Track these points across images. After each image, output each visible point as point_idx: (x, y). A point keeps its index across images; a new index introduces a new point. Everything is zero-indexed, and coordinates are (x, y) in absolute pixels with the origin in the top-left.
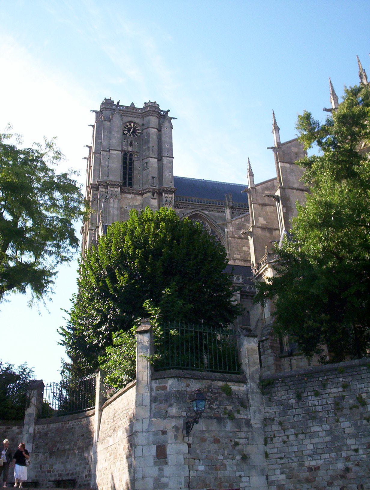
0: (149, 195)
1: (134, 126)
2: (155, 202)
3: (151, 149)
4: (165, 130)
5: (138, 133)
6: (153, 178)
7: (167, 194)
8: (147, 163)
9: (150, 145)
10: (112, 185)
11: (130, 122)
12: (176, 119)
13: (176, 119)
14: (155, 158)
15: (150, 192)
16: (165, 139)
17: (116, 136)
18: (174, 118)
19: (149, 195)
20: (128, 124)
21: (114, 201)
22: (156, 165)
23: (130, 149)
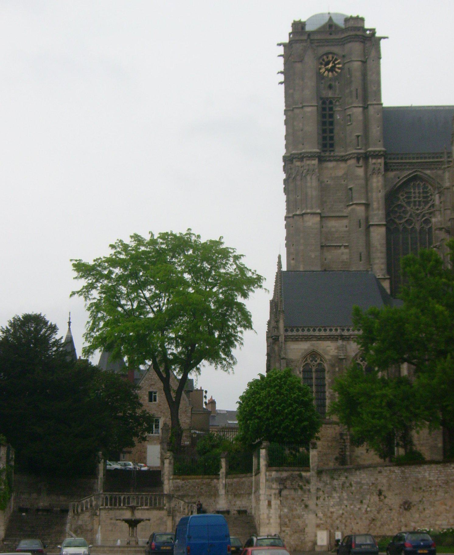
0: (352, 162)
1: (333, 58)
2: (360, 172)
3: (354, 93)
4: (370, 64)
5: (339, 68)
6: (358, 136)
7: (375, 158)
8: (349, 115)
9: (353, 88)
10: (307, 157)
11: (327, 54)
12: (387, 38)
13: (387, 38)
14: (360, 107)
15: (354, 158)
16: (370, 77)
17: (311, 83)
18: (384, 38)
19: (352, 162)
20: (325, 57)
21: (311, 178)
22: (361, 118)
23: (330, 94)
